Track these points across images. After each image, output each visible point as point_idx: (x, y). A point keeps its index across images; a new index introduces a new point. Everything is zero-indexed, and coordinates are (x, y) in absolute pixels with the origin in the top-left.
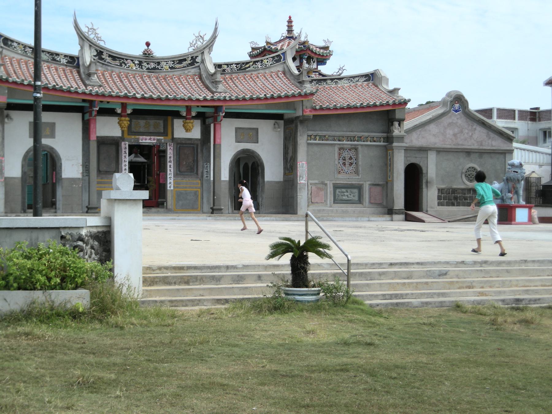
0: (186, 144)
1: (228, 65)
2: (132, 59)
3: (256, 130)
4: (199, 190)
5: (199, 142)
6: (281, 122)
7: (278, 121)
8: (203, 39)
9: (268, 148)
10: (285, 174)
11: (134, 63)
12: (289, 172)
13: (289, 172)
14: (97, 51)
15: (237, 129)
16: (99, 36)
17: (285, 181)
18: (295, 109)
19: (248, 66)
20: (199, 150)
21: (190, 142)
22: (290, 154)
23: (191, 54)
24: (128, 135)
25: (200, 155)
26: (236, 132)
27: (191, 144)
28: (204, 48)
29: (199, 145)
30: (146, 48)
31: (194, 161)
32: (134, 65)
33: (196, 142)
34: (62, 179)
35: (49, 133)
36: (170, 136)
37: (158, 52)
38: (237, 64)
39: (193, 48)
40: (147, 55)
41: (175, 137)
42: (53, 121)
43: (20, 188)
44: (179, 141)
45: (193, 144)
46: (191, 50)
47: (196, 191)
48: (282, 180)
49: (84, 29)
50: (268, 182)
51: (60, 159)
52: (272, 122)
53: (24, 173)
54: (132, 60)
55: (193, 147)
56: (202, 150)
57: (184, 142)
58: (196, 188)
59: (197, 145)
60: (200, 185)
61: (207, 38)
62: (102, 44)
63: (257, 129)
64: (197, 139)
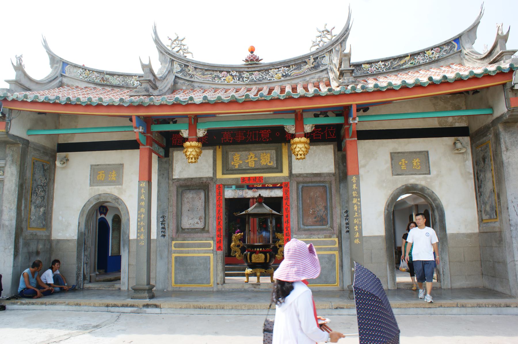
0: (312, 182)
1: (370, 63)
2: (228, 70)
3: (426, 154)
4: (336, 253)
5: (333, 178)
6: (466, 140)
7: (460, 138)
8: (331, 34)
9: (449, 176)
10: (481, 220)
11: (231, 75)
12: (490, 218)
13: (490, 218)
14: (181, 66)
15: (394, 156)
16: (185, 47)
17: (481, 233)
18: (491, 108)
19: (402, 62)
20: (333, 191)
21: (318, 179)
22: (489, 186)
23: (313, 55)
24: (223, 174)
25: (336, 199)
26: (392, 159)
27: (320, 182)
28: (333, 45)
29: (333, 183)
30: (249, 54)
31: (326, 208)
32: (231, 77)
33: (327, 179)
34: (129, 240)
35: (114, 179)
36: (286, 173)
37: (267, 57)
38: (385, 61)
39: (317, 47)
40: (253, 62)
41: (294, 172)
42: (118, 162)
43: (75, 253)
44: (301, 179)
45: (323, 182)
46: (314, 49)
47: (331, 255)
48: (477, 230)
49: (166, 43)
50: (453, 234)
51: (83, 211)
52: (449, 141)
53: (81, 235)
54: (228, 72)
55: (325, 187)
56: (338, 190)
57: (308, 180)
58: (331, 249)
59: (331, 184)
60: (337, 245)
61: (337, 32)
62: (189, 57)
63: (427, 152)
64: (329, 174)
